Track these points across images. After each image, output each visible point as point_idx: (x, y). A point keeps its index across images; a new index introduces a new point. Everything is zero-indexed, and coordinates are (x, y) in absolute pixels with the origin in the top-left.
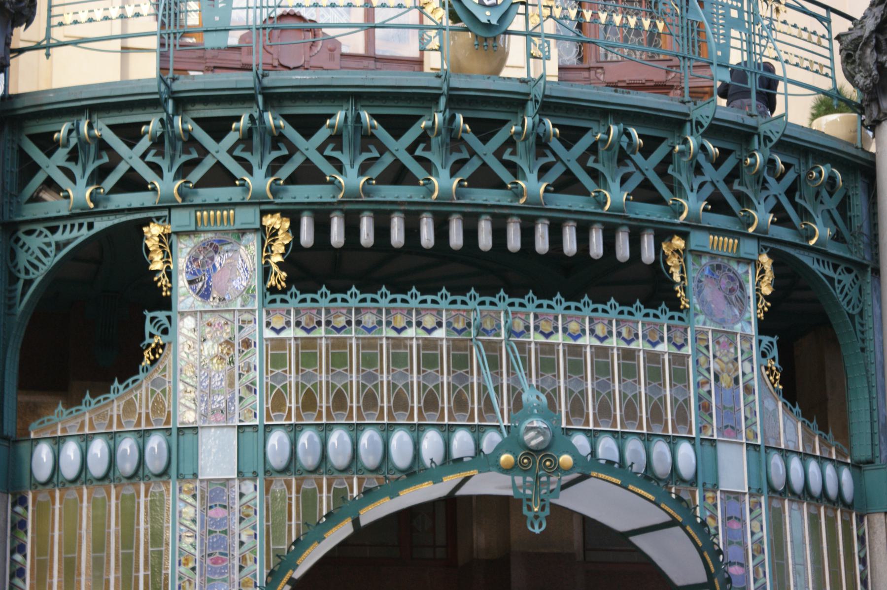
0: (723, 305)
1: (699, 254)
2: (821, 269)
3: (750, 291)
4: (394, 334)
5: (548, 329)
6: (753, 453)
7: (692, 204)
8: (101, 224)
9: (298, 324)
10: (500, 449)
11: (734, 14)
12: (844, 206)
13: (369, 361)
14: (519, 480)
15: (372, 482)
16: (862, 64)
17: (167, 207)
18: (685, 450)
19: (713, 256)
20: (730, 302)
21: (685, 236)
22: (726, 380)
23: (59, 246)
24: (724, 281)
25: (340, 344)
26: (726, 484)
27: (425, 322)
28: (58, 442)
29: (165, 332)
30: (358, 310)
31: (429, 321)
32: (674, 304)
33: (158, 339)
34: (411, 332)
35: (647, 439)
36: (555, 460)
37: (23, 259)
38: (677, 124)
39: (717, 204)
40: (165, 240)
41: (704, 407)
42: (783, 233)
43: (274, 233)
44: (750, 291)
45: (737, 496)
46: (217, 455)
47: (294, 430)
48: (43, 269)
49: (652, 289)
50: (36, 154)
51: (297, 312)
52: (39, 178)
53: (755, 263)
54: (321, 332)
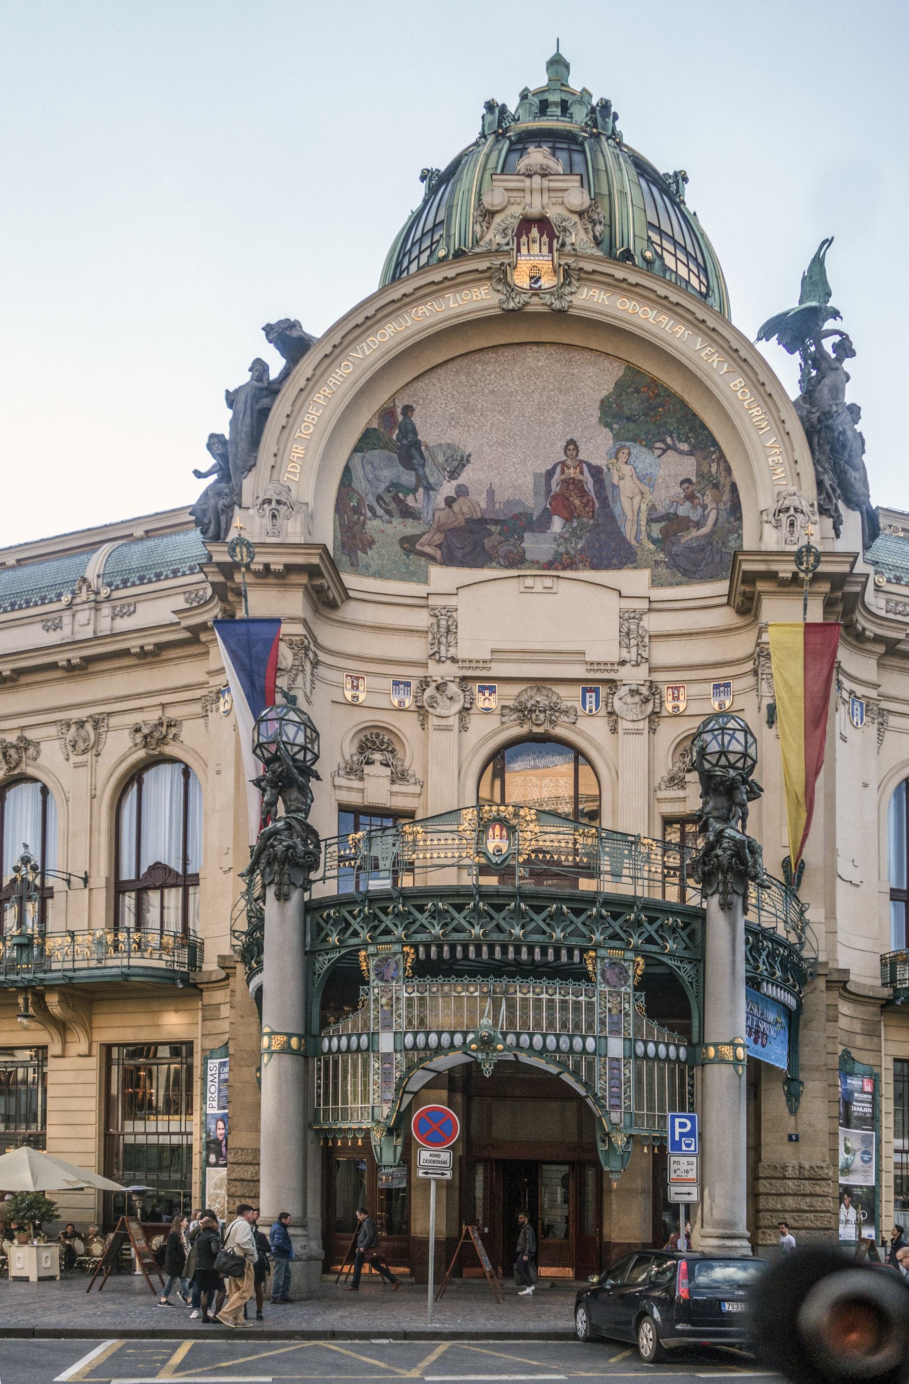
0: (615, 979)
1: (603, 958)
3: (631, 973)
6: (627, 1042)
11: (626, 852)
12: (691, 936)
18: (591, 1044)
20: (620, 980)
21: (595, 950)
22: (614, 1011)
26: (610, 1054)
32: (589, 980)
35: (571, 1037)
41: (603, 1023)
44: (631, 973)
49: (580, 975)
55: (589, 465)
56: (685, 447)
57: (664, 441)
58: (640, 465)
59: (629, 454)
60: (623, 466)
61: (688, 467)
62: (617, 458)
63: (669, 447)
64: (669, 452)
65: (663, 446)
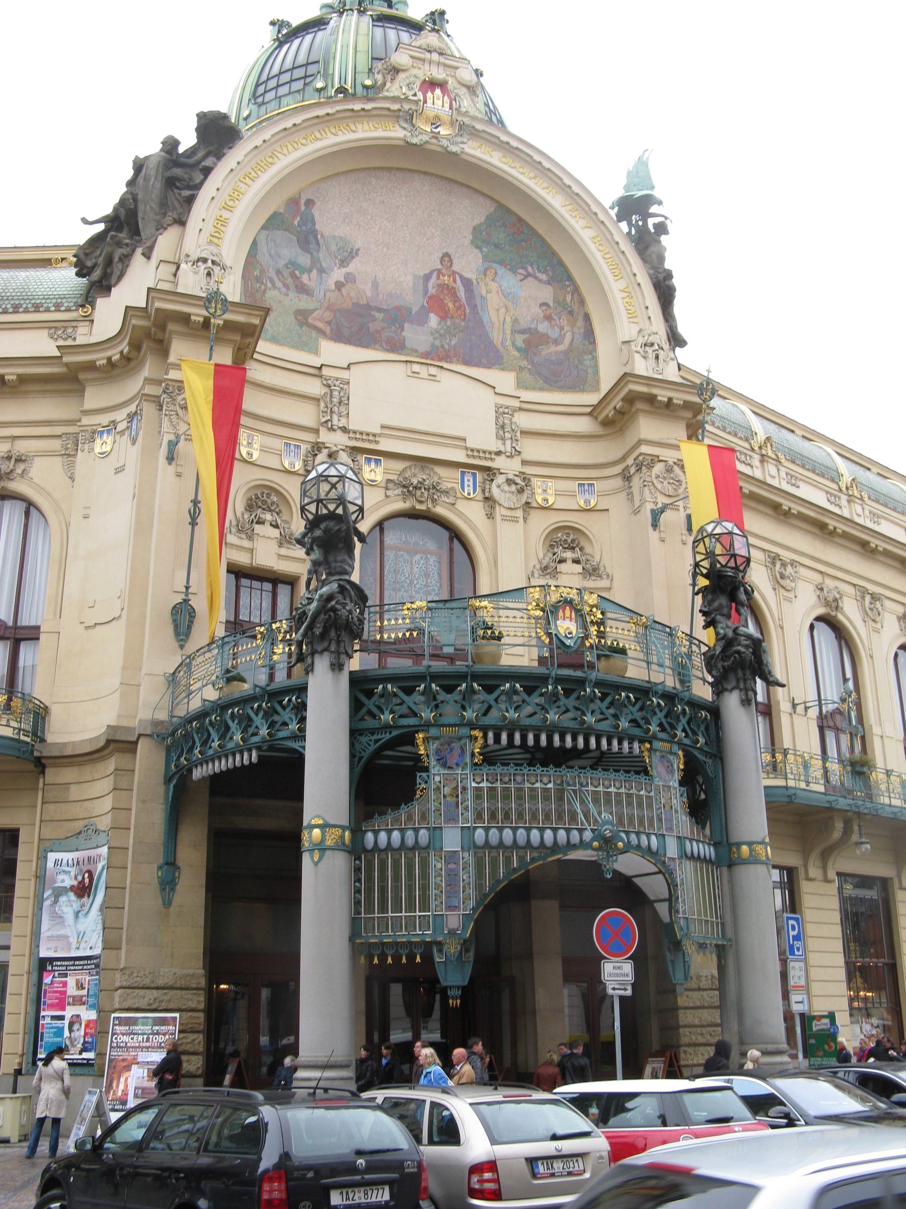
1: (656, 750)
2: (701, 757)
3: (675, 767)
4: (530, 786)
5: (596, 784)
7: (654, 728)
8: (395, 733)
9: (487, 780)
10: (593, 840)
13: (520, 797)
14: (600, 853)
15: (535, 854)
16: (716, 666)
17: (427, 726)
18: (653, 838)
19: (661, 751)
20: (668, 772)
21: (650, 743)
23: (376, 741)
24: (666, 764)
25: (506, 790)
27: (543, 781)
28: (376, 833)
29: (426, 782)
30: (514, 775)
31: (545, 780)
32: (646, 773)
33: (423, 786)
34: (538, 785)
35: (638, 834)
36: (616, 845)
37: (358, 747)
38: (582, 682)
39: (663, 729)
40: (426, 740)
41: (660, 819)
42: (687, 741)
43: (476, 738)
44: (675, 767)
45: (673, 859)
46: (451, 840)
47: (487, 829)
48: (368, 752)
50: (364, 699)
51: (487, 775)
52: (364, 710)
53: (675, 754)
54: (498, 784)
55: (461, 277)
56: (544, 277)
57: (526, 270)
58: (505, 285)
59: (496, 273)
60: (490, 283)
61: (547, 294)
62: (485, 275)
63: (529, 275)
64: (530, 279)
65: (524, 272)
